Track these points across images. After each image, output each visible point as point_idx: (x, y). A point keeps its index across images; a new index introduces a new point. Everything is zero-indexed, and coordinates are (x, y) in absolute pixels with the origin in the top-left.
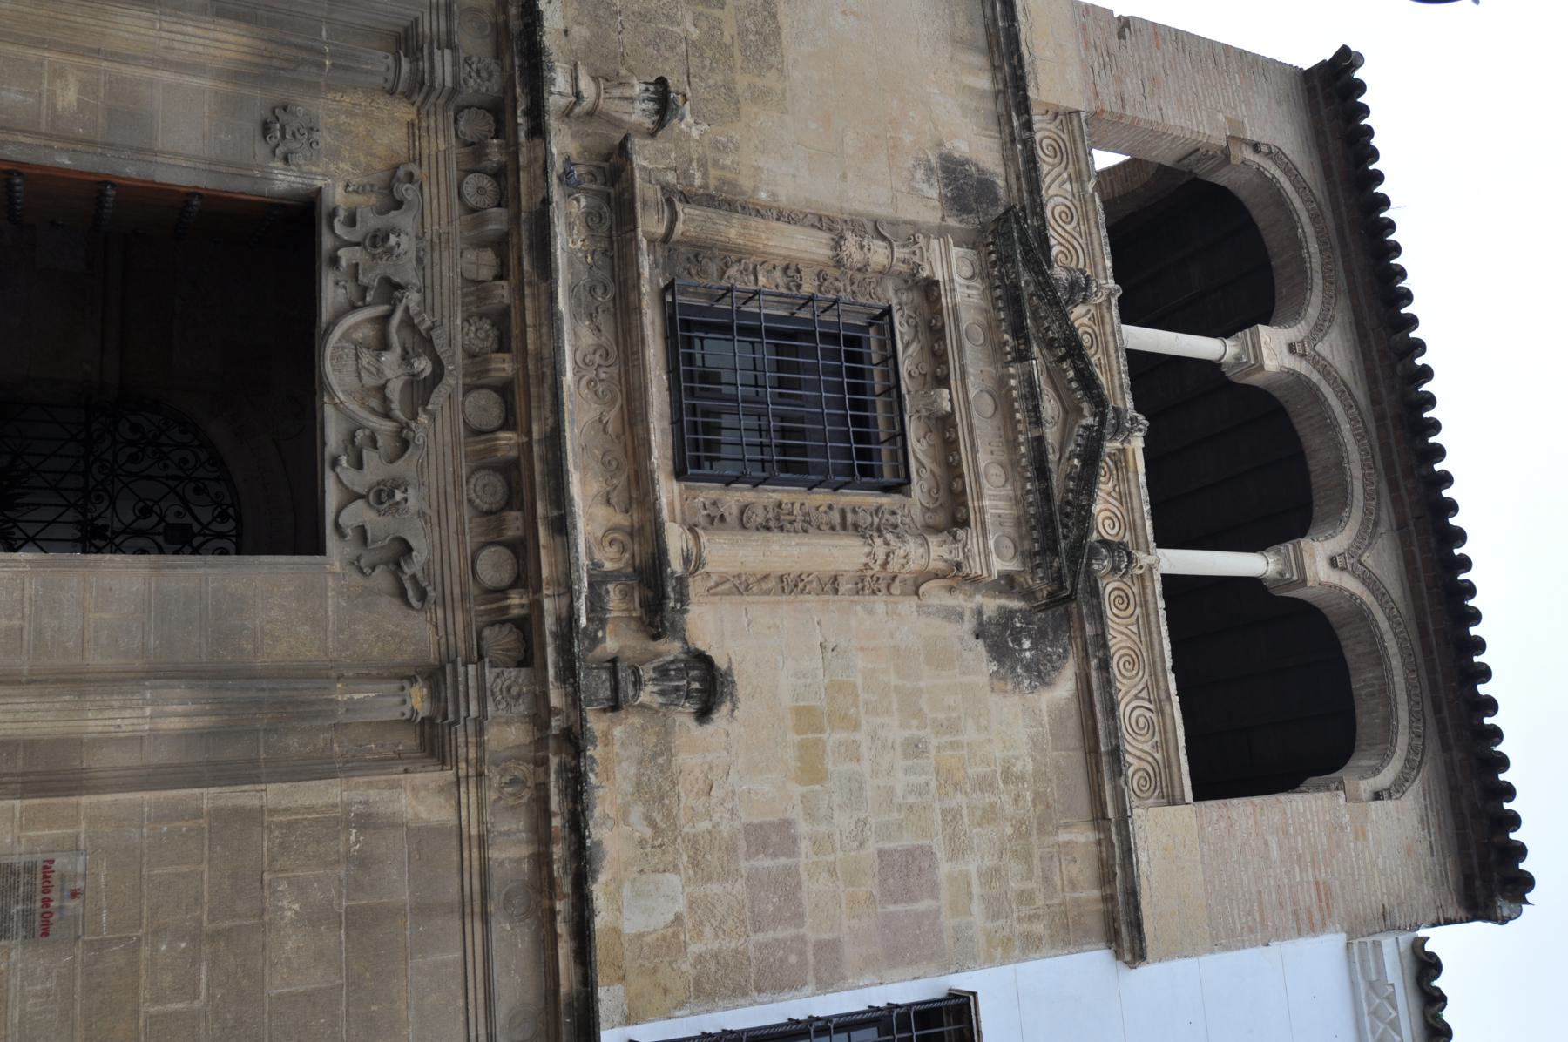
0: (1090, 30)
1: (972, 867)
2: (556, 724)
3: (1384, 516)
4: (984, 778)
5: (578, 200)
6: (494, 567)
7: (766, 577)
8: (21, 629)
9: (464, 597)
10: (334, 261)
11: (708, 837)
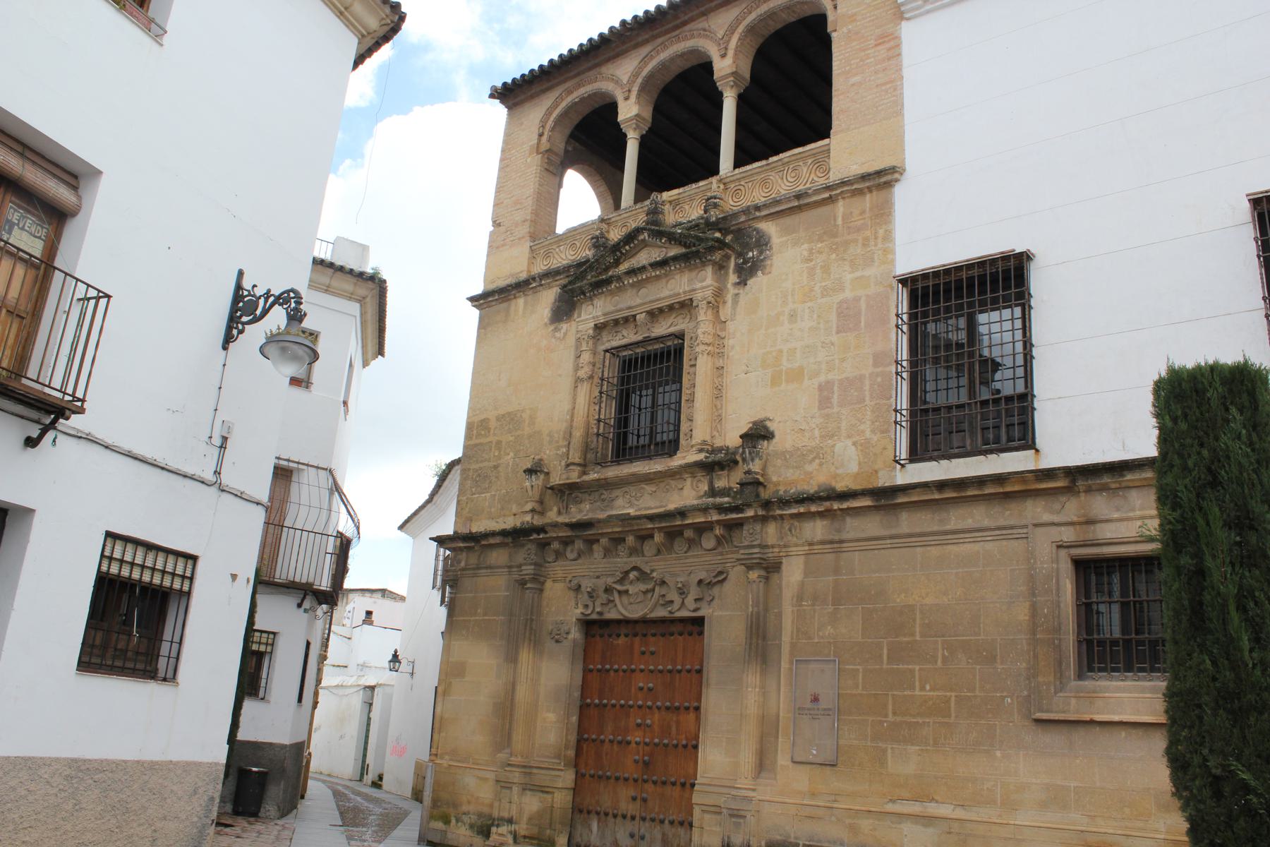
2: (760, 512)
6: (708, 542)
9: (721, 554)
10: (600, 613)
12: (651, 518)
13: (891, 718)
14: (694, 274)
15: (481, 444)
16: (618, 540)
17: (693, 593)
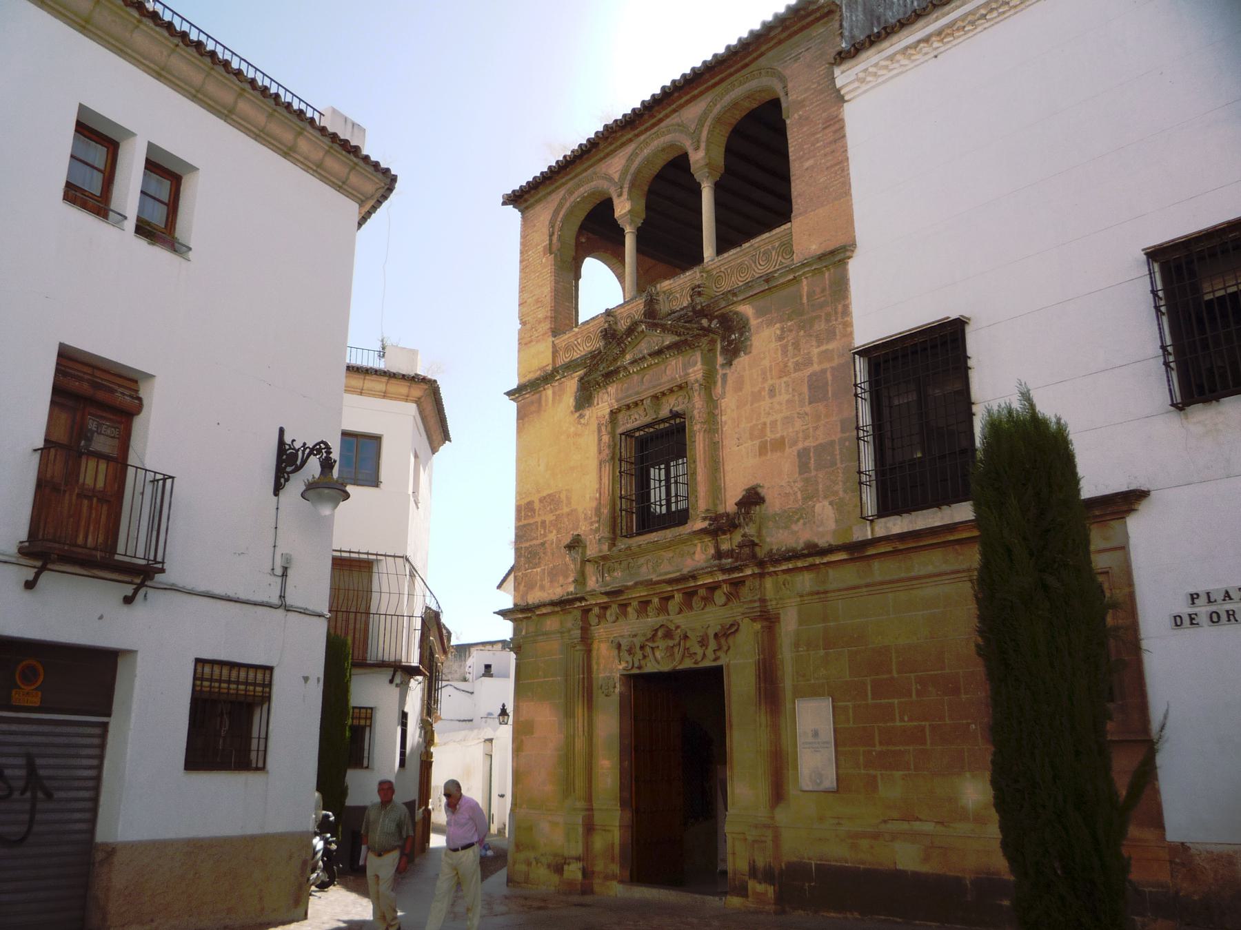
1: (816, 351)
2: (757, 571)
3: (674, 121)
6: (719, 597)
12: (670, 582)
13: (878, 748)
15: (529, 524)
16: (645, 604)
17: (713, 644)
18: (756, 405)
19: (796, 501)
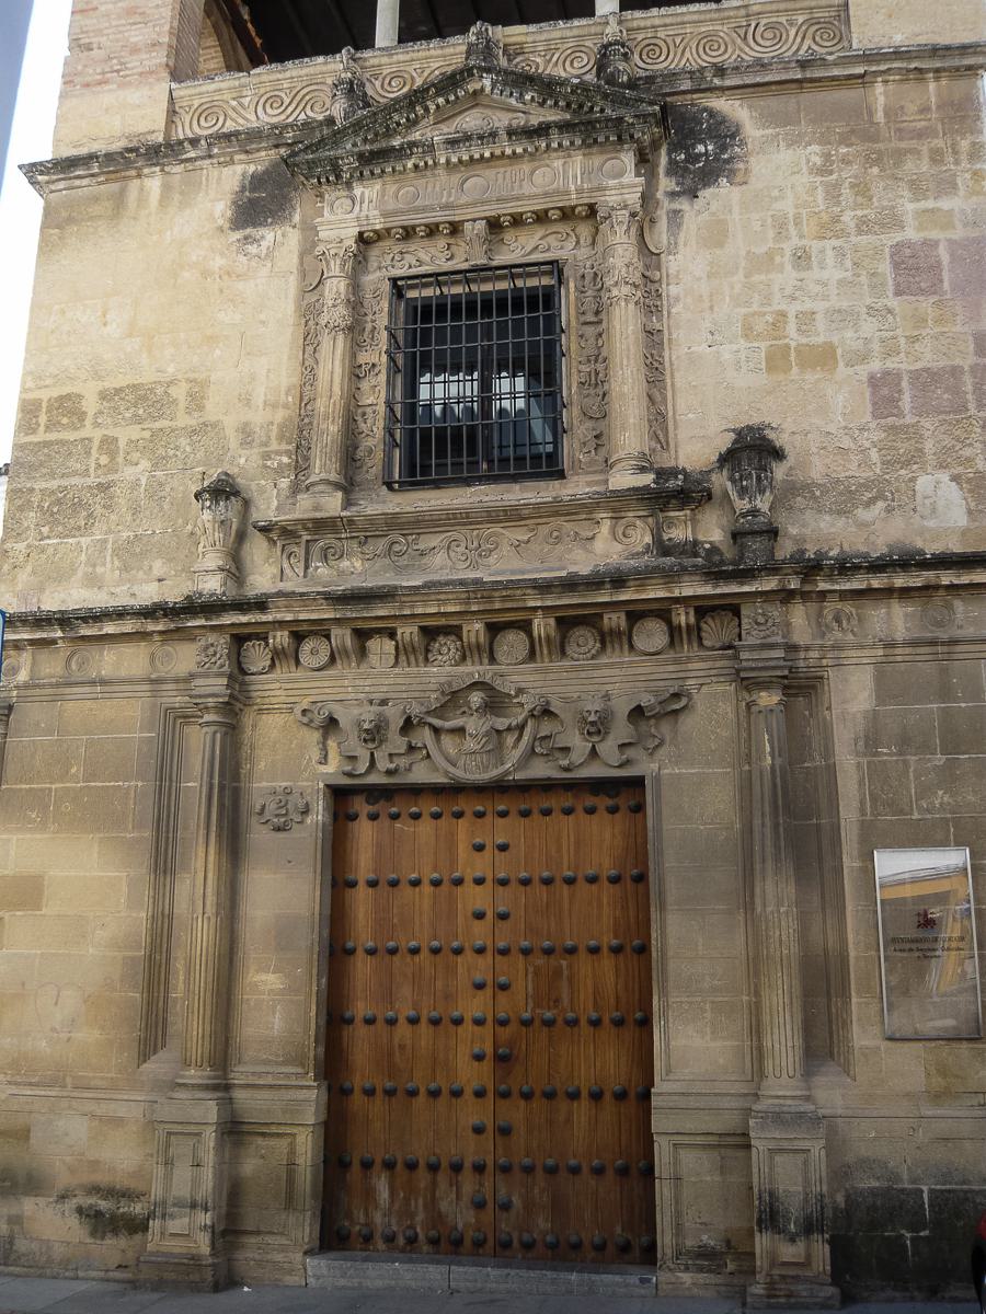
0: (89, 79)
1: (910, 207)
4: (827, 193)
5: (317, 568)
6: (652, 636)
7: (649, 396)
8: (713, 1002)
9: (676, 662)
10: (389, 773)
11: (883, 452)
12: (544, 587)
14: (597, 160)
15: (62, 443)
18: (756, 278)
19: (865, 463)
